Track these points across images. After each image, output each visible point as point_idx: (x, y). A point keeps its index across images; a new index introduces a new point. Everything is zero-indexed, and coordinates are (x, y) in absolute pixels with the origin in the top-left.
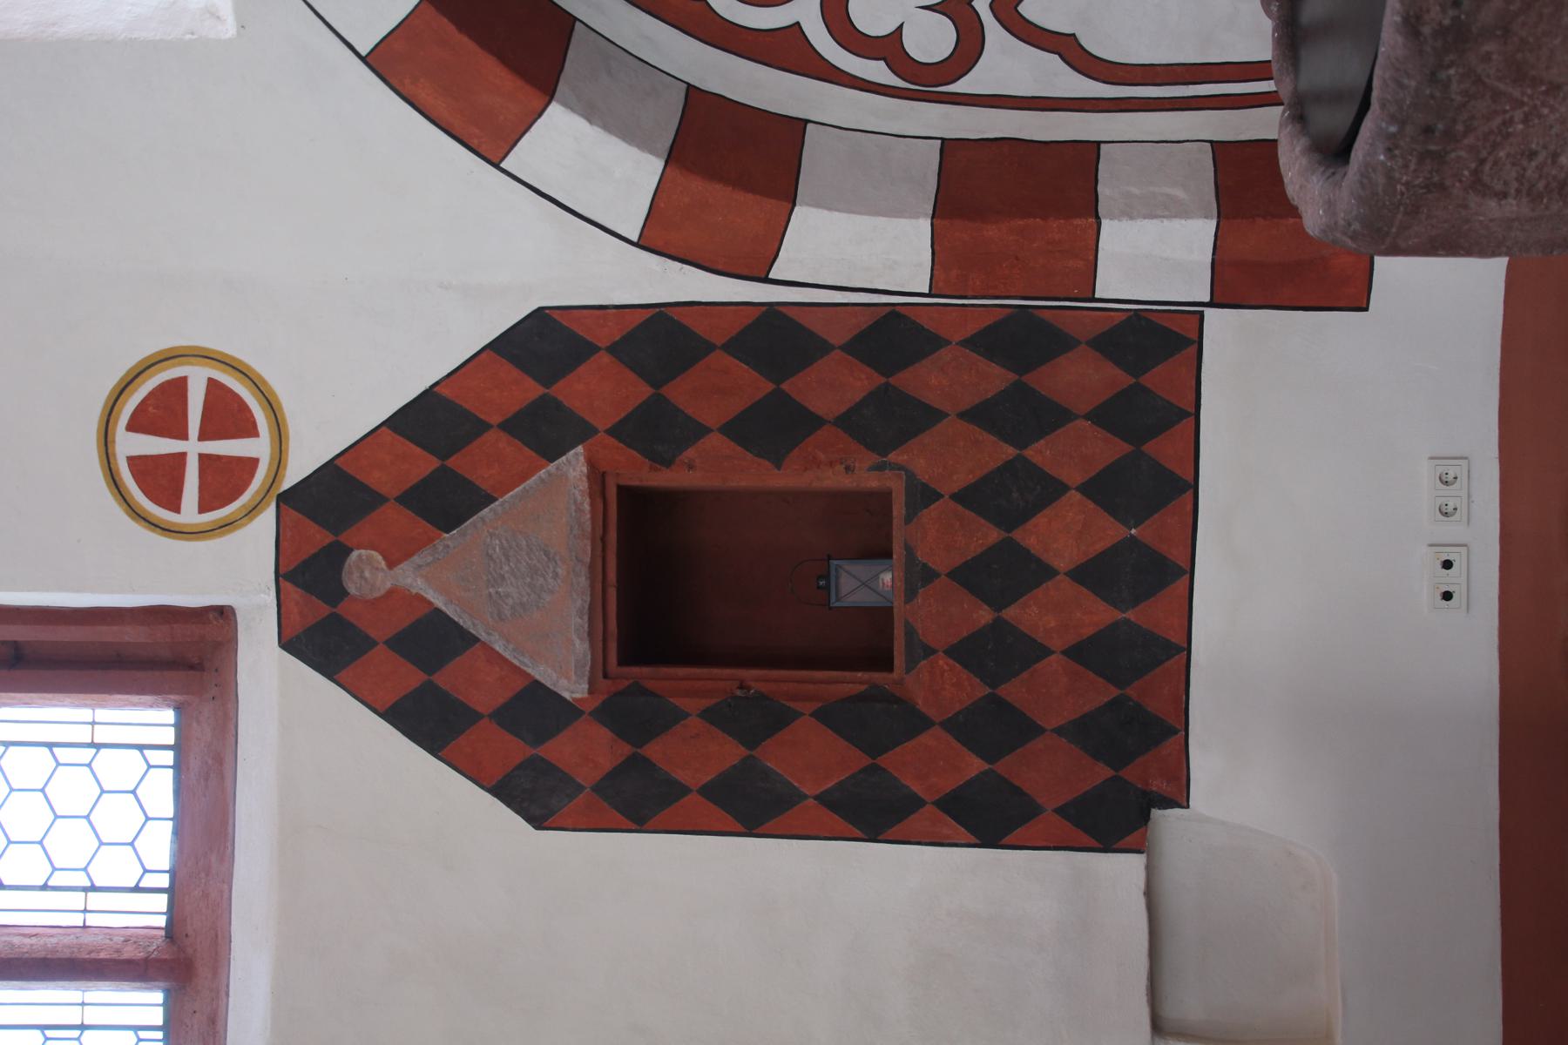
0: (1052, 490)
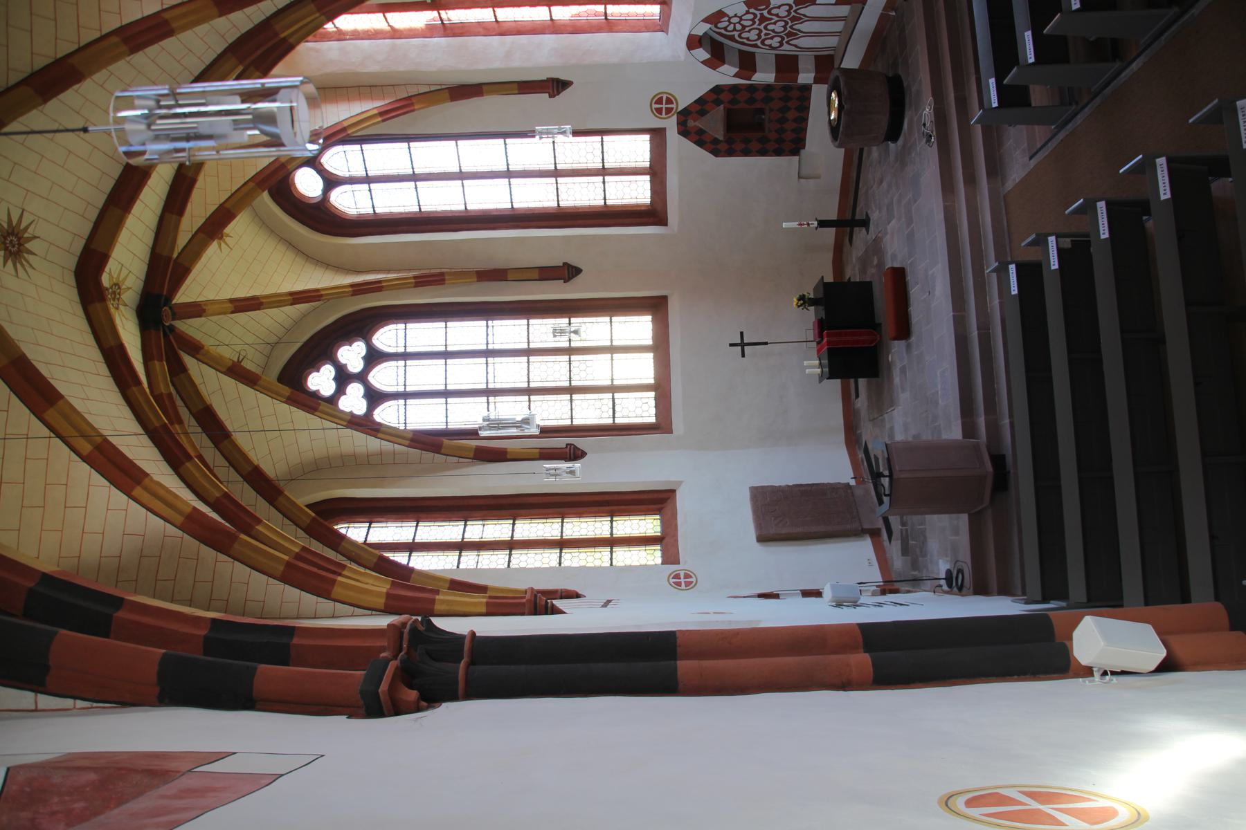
0: (789, 109)
